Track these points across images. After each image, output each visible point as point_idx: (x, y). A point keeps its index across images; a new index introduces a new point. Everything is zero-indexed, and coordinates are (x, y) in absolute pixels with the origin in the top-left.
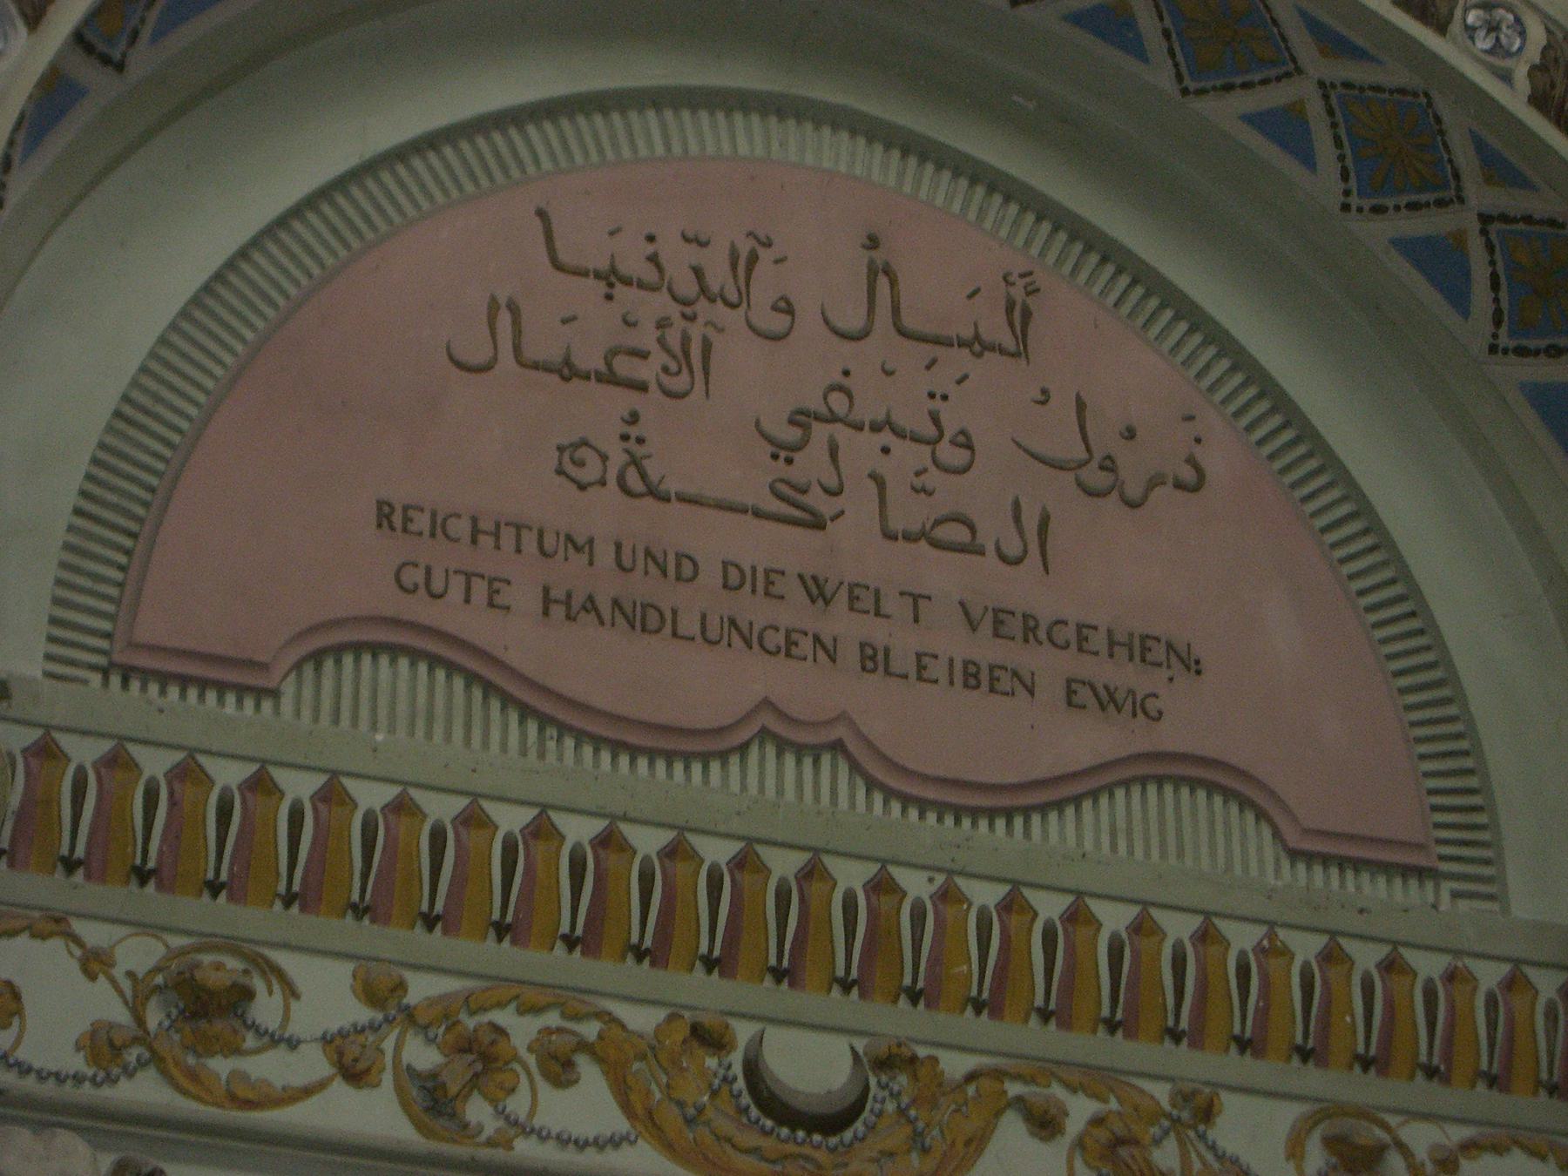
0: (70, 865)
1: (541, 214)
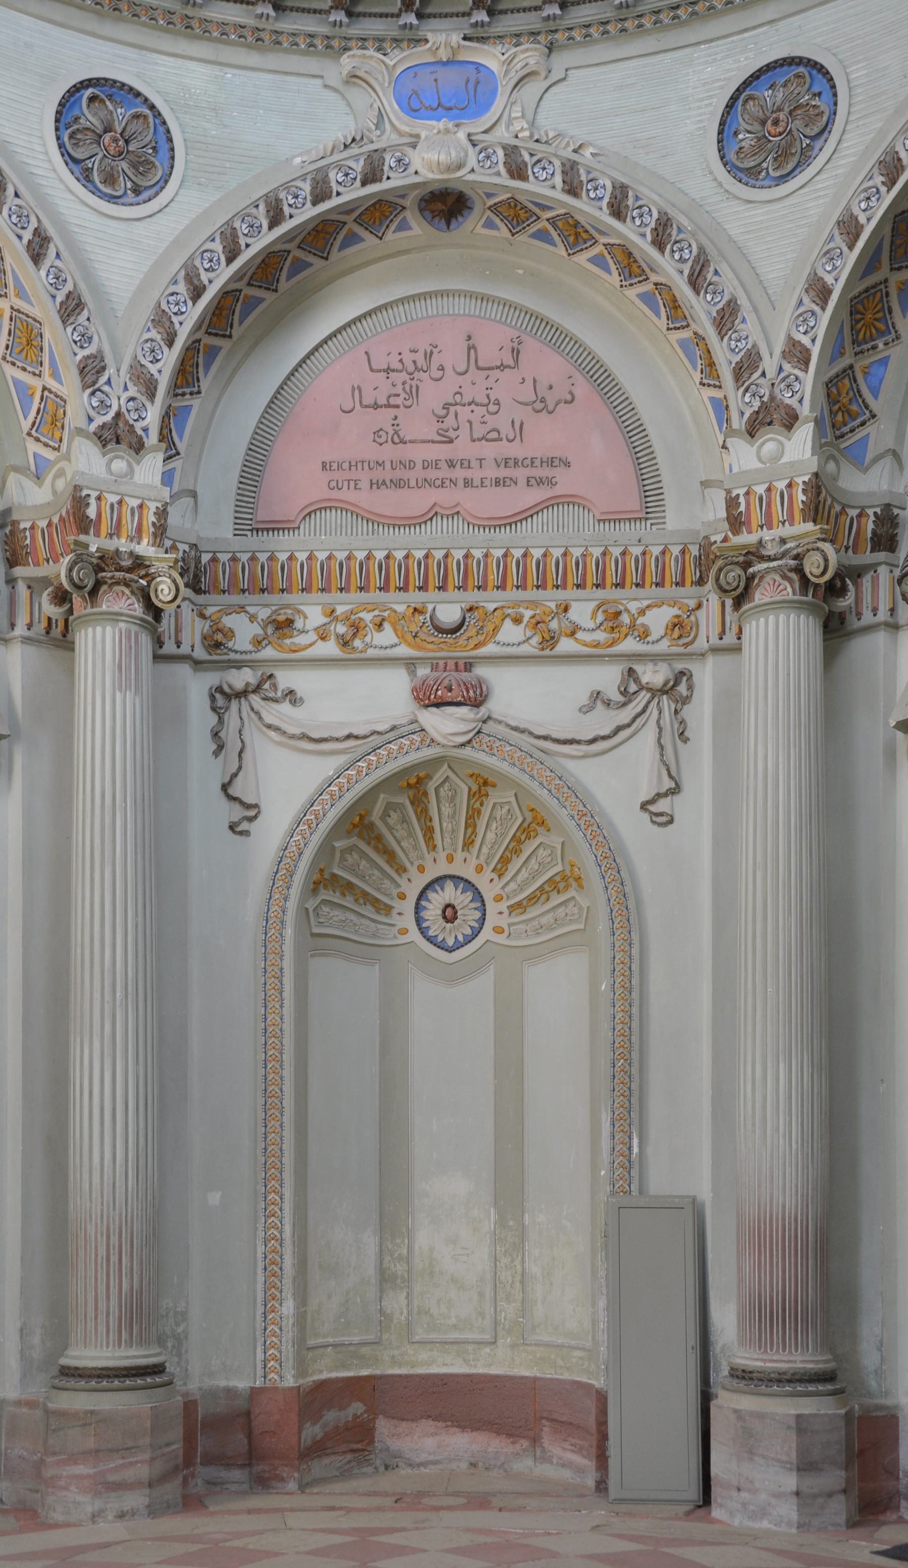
0: (243, 591)
1: (366, 353)
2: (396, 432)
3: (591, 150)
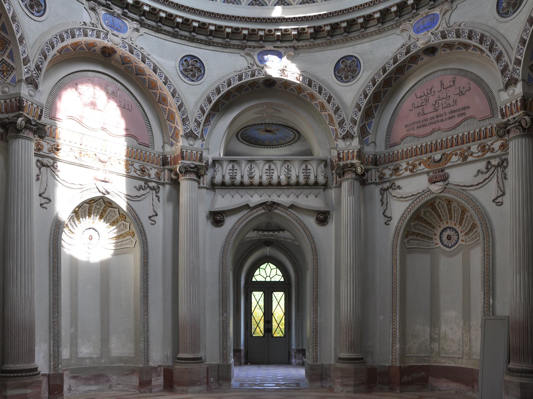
1: (415, 94)
2: (423, 112)
3: (463, 24)
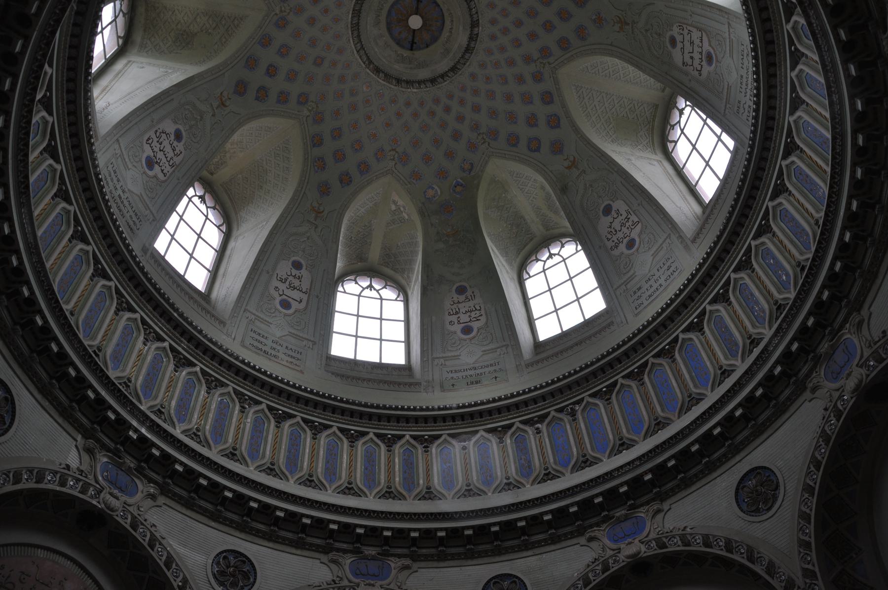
3: (689, 527)
